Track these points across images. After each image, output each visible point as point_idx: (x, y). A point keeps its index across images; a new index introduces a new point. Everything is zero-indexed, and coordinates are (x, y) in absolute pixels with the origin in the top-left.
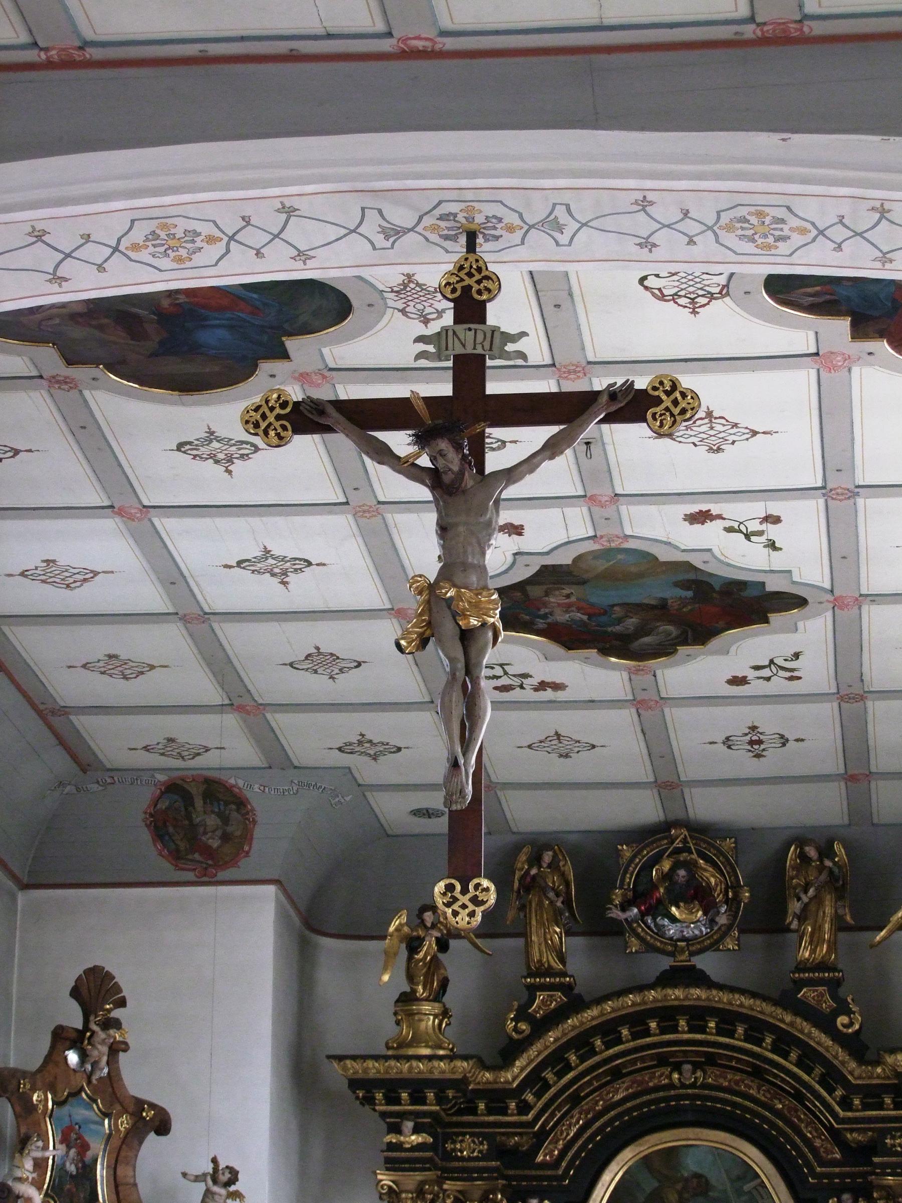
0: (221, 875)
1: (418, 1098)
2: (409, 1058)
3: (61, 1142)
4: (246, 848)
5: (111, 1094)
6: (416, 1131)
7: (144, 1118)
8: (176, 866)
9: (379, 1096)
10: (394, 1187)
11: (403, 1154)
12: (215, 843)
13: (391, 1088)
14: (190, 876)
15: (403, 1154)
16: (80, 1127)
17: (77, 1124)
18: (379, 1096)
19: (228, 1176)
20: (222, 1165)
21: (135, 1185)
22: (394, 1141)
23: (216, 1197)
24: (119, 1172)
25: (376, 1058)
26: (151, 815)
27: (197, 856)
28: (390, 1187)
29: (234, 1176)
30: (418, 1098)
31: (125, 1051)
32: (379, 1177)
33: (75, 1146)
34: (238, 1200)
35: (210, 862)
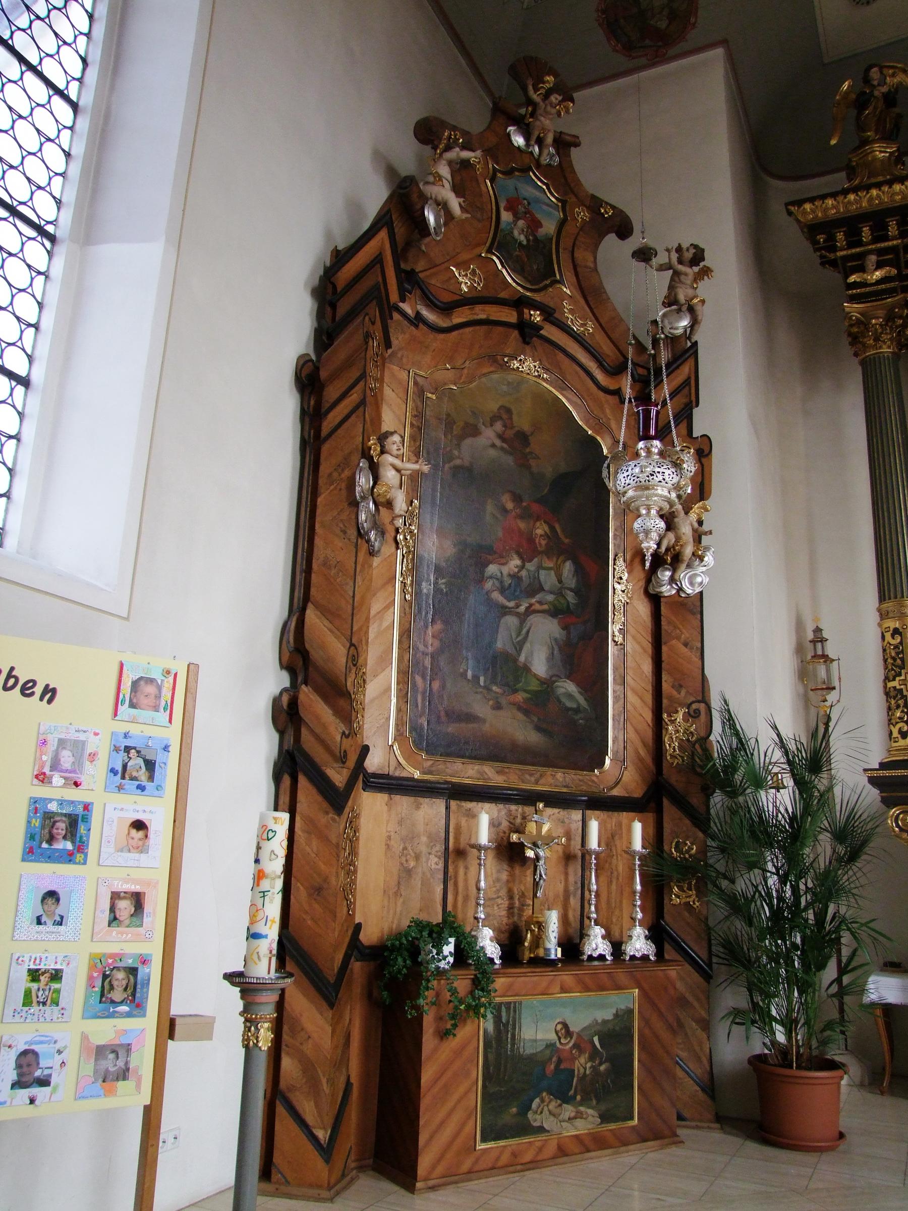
0: (672, 52)
1: (880, 234)
2: (868, 188)
3: (506, 209)
4: (693, 20)
5: (563, 178)
6: (879, 266)
7: (603, 215)
8: (630, 56)
9: (840, 236)
10: (862, 319)
11: (868, 289)
12: (663, 25)
13: (851, 224)
14: (643, 61)
15: (868, 289)
16: (529, 203)
17: (525, 199)
18: (840, 236)
19: (692, 251)
20: (685, 246)
21: (595, 269)
22: (858, 280)
23: (682, 277)
24: (576, 255)
25: (834, 195)
26: (603, 12)
27: (647, 42)
28: (857, 319)
29: (698, 256)
30: (880, 234)
31: (577, 145)
32: (847, 310)
33: (524, 218)
34: (706, 277)
35: (660, 44)
